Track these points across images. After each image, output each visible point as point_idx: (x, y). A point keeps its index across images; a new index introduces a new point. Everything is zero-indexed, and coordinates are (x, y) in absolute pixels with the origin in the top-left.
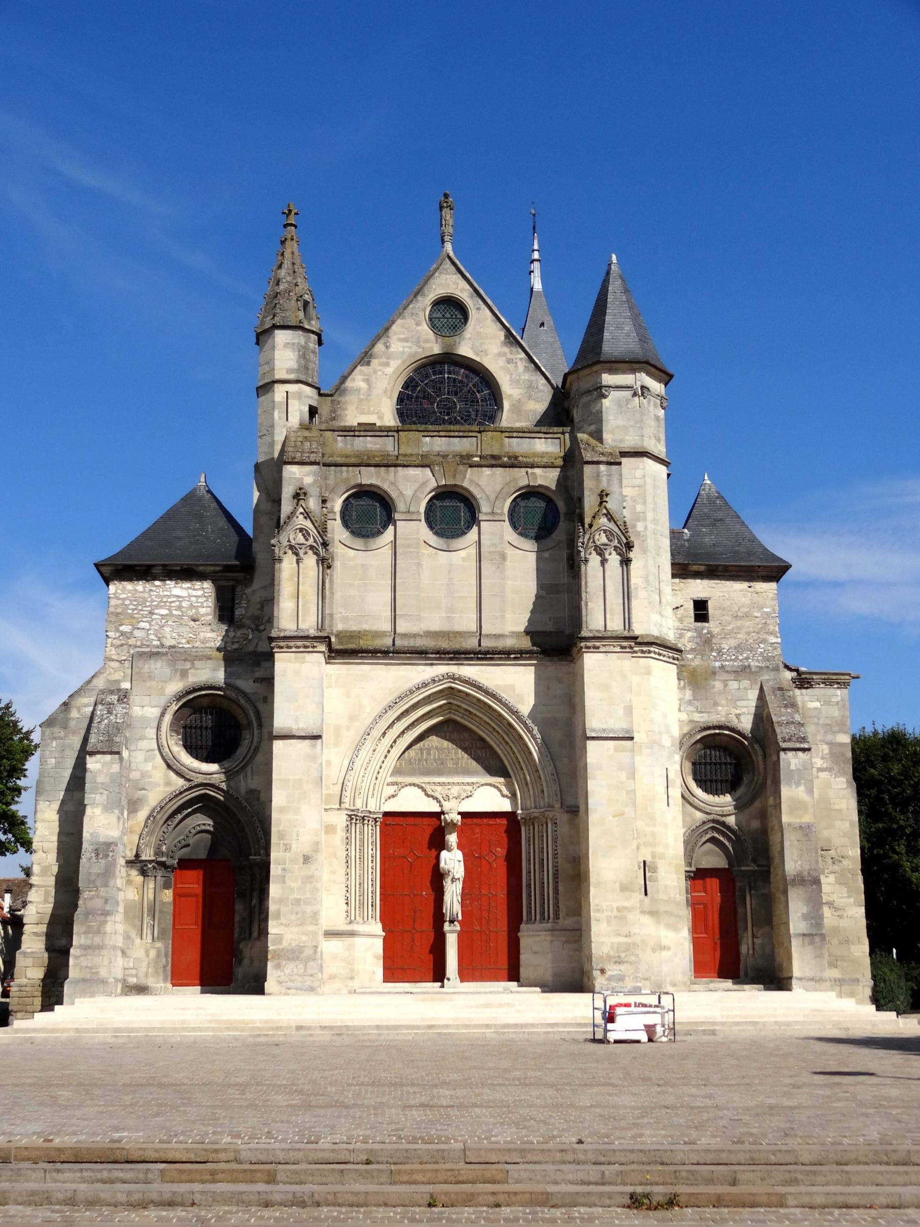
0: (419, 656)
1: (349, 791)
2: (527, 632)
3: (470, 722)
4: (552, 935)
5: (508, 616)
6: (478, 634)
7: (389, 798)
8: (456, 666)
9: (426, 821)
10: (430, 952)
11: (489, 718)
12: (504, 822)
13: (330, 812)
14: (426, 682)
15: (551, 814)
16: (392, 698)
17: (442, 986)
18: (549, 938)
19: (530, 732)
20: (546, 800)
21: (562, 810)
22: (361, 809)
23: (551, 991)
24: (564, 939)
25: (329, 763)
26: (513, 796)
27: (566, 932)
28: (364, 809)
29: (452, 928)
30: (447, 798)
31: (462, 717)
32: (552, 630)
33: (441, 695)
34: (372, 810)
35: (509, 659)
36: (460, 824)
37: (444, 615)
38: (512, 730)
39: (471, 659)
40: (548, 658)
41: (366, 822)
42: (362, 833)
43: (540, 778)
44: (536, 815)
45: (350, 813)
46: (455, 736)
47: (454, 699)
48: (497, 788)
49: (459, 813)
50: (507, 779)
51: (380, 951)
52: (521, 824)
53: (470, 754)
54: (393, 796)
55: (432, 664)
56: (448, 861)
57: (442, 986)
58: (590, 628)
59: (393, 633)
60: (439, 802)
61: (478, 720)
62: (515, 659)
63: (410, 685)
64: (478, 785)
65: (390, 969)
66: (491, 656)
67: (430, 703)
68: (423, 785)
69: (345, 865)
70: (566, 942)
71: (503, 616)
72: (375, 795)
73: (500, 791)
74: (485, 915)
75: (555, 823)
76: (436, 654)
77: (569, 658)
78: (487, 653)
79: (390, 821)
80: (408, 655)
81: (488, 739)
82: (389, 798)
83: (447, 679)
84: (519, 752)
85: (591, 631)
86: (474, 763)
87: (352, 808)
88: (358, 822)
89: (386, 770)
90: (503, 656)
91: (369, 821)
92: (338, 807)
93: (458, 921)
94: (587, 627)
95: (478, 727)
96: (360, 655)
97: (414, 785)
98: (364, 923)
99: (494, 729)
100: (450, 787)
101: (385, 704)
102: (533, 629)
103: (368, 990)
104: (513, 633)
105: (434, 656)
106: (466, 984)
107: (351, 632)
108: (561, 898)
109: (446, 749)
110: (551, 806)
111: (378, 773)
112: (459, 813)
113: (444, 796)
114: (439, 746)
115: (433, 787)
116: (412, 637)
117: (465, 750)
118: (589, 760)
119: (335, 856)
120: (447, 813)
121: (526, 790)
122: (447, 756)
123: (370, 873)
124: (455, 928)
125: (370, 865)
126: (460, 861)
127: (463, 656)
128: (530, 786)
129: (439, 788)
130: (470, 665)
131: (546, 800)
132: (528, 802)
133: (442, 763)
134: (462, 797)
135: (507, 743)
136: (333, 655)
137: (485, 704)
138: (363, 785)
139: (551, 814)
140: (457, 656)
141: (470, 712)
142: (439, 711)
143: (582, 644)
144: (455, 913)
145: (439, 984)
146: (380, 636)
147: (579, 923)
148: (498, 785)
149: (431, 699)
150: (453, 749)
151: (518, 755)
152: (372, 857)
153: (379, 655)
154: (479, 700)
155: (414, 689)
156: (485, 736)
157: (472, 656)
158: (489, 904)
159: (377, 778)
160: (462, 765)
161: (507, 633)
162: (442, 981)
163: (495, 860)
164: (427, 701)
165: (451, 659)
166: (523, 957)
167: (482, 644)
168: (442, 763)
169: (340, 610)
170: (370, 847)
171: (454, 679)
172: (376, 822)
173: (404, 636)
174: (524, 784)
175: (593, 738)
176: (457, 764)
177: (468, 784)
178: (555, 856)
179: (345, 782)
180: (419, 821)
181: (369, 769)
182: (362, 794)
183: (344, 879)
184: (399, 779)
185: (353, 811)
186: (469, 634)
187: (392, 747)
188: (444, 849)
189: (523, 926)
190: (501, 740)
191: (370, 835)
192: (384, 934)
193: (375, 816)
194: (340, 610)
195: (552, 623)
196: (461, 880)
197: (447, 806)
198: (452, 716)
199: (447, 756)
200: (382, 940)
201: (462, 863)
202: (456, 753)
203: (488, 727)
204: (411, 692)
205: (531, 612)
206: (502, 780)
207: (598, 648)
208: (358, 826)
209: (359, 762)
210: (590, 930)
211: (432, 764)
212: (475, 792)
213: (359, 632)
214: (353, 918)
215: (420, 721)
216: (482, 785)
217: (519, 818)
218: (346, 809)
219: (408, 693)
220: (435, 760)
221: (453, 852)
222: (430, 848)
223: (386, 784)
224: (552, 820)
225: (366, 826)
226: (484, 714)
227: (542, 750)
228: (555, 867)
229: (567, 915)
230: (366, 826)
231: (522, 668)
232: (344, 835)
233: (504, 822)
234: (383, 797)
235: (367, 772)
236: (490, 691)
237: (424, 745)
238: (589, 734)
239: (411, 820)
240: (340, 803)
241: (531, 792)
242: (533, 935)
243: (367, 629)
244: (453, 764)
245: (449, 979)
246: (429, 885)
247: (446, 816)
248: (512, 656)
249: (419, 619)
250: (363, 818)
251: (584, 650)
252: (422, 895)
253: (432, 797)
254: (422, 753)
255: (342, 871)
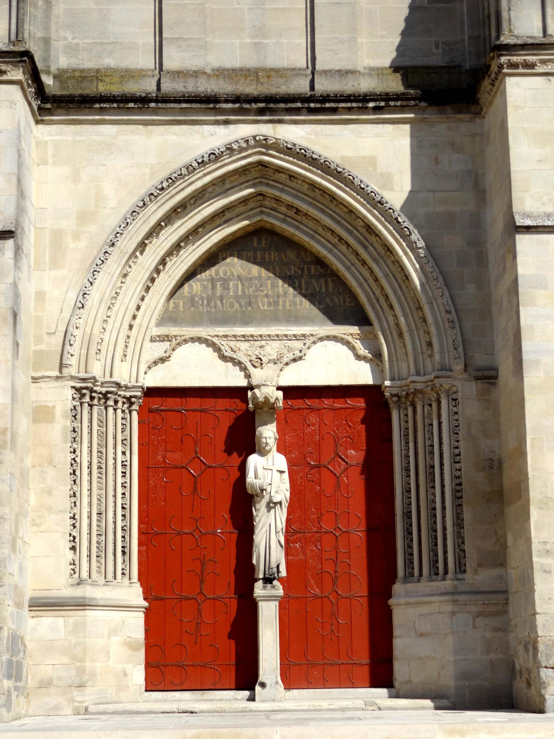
0: (203, 106)
1: (77, 345)
2: (396, 68)
3: (297, 228)
4: (455, 602)
5: (363, 40)
6: (309, 72)
7: (155, 363)
8: (270, 126)
9: (222, 403)
10: (231, 636)
11: (333, 218)
12: (361, 403)
13: (42, 384)
14: (217, 152)
15: (446, 384)
16: (155, 181)
17: (252, 699)
18: (448, 608)
19: (405, 236)
20: (437, 357)
21: (466, 376)
22: (101, 379)
23: (454, 707)
24: (474, 609)
25: (40, 296)
26: (377, 356)
27: (480, 597)
28: (108, 379)
29: (269, 591)
30: (259, 362)
31: (283, 221)
32: (440, 63)
33: (243, 179)
34: (123, 383)
35: (364, 110)
36: (281, 404)
37: (248, 40)
38: (373, 238)
39: (297, 111)
40: (434, 109)
41: (111, 403)
42: (103, 423)
43: (424, 320)
44: (419, 386)
45: (78, 385)
46: (273, 255)
47: (268, 185)
48: (347, 344)
49: (279, 388)
50: (366, 328)
51: (139, 634)
52: (392, 405)
53: (298, 288)
54: (163, 360)
55: (227, 123)
56: (260, 472)
57: (252, 699)
58: (516, 32)
59: (157, 72)
60: (244, 369)
61: (311, 224)
62: (377, 110)
63: (189, 157)
64: (312, 339)
65: (157, 667)
66: (332, 105)
67: (225, 193)
68: (215, 340)
69: (69, 480)
70: (480, 614)
71: (353, 39)
72: (129, 358)
73: (353, 349)
74: (329, 568)
75: (455, 400)
76: (234, 102)
77: (473, 108)
78: (326, 98)
79: (156, 403)
80: (184, 105)
81: (331, 259)
82: (155, 363)
83: (254, 147)
84: (386, 276)
85: (517, 37)
86: (306, 303)
87: (83, 375)
88: (96, 402)
89: (149, 314)
90: (354, 105)
91: (116, 402)
92: (57, 373)
93: (281, 580)
94: (510, 31)
95: (312, 237)
96: (97, 106)
97: (200, 340)
98: (107, 583)
99: (341, 239)
100: (263, 343)
101: (143, 191)
102: (407, 62)
103: (111, 708)
104: (371, 69)
105: (230, 106)
106: (295, 692)
107: (83, 71)
108: (467, 533)
109: (255, 278)
110: (445, 368)
111: (134, 317)
112: (279, 388)
113: (253, 358)
114: (243, 273)
115: (232, 344)
116: (191, 76)
117: (289, 280)
118: (521, 270)
119: (51, 462)
120: (258, 387)
121: (399, 344)
122: (257, 290)
123: (119, 496)
124: (273, 592)
125: (120, 480)
126: (282, 472)
127: (282, 105)
128: (406, 336)
129: (244, 346)
130: (295, 122)
131: (437, 357)
132: (404, 366)
133: (250, 304)
134: (285, 360)
135: (364, 263)
136: (49, 106)
137: (324, 191)
138: (106, 337)
139: (446, 384)
140: (272, 105)
141: (298, 211)
142: (242, 209)
143: (503, 59)
144: (274, 565)
145: (247, 693)
146: (133, 77)
147: (501, 579)
148: (350, 339)
149: (228, 185)
150: (269, 278)
151: (384, 282)
152: (124, 466)
153: (131, 105)
154: (313, 185)
155: (195, 164)
156: (323, 252)
157: (299, 105)
158: (336, 548)
159: (131, 327)
160: (284, 305)
161: (362, 71)
162: (251, 688)
163: (346, 469)
164: (218, 190)
165: (261, 112)
166: (398, 644)
167: (317, 87)
168: (250, 304)
169: (62, 33)
170: (120, 449)
171: (268, 147)
172: (132, 404)
173: (178, 74)
174: (395, 336)
175: (528, 229)
176: (276, 304)
177: (296, 337)
178: (456, 458)
179: (71, 328)
180: (209, 403)
181: (115, 309)
182: (103, 352)
183: (67, 503)
184: (173, 330)
185: (84, 380)
186: (295, 72)
187: (158, 271)
188: (253, 451)
189: (397, 588)
190: (354, 259)
191: (119, 427)
192: (146, 604)
193: (128, 394)
194: (62, 33)
195: (440, 51)
196: (285, 505)
197: (258, 375)
198: (265, 218)
199: (257, 290)
200: (142, 615)
201: (286, 476)
202: (274, 286)
203: (329, 235)
204: (190, 169)
205: (404, 34)
206: (355, 330)
207: (532, 66)
208: (95, 409)
209: (95, 294)
210: (532, 591)
211: (232, 306)
212: (309, 352)
213: (98, 71)
214: (85, 575)
215: (208, 227)
216: (321, 339)
217: (387, 394)
218: (73, 378)
219: (184, 171)
220: (237, 298)
221: (270, 456)
222: (228, 451)
223: (148, 338)
224: (448, 393)
225: (111, 410)
226: (323, 212)
227: (428, 269)
228: (457, 479)
229: (480, 565)
230: (111, 410)
231: (389, 127)
232: (69, 424)
233: (361, 403)
234: (143, 360)
235: (112, 313)
236: (332, 166)
237: (217, 273)
238: (520, 221)
239: (194, 403)
240: (62, 366)
241: (409, 347)
242: (417, 603)
243: (112, 66)
244: (269, 304)
245: (263, 685)
246: (227, 516)
247: (256, 391)
248: (371, 105)
249: (205, 47)
250: (105, 396)
251: (505, 71)
252: (215, 534)
253: (232, 360)
254: (214, 287)
255: (65, 488)
